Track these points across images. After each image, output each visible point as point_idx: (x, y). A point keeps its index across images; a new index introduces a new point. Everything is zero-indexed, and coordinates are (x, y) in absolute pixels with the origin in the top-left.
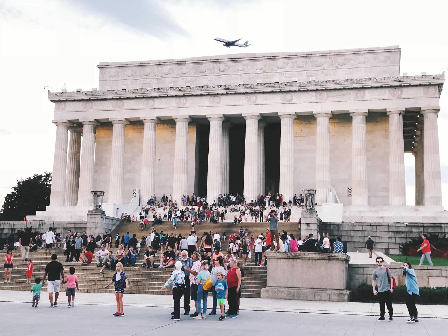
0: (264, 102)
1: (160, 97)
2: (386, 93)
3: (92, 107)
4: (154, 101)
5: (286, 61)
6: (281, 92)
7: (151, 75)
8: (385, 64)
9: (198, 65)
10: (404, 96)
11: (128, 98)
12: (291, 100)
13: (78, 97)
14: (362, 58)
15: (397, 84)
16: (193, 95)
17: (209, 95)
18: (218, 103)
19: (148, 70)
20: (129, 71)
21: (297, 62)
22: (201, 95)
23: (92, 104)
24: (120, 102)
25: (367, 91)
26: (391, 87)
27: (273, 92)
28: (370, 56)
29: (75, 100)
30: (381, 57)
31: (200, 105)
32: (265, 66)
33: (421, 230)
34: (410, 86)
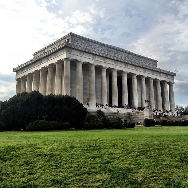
0: (139, 70)
1: (111, 59)
3: (83, 55)
4: (107, 60)
5: (133, 56)
7: (92, 46)
9: (108, 48)
11: (99, 56)
14: (150, 62)
15: (168, 73)
16: (121, 62)
17: (126, 63)
19: (91, 43)
24: (95, 56)
28: (151, 61)
31: (122, 66)
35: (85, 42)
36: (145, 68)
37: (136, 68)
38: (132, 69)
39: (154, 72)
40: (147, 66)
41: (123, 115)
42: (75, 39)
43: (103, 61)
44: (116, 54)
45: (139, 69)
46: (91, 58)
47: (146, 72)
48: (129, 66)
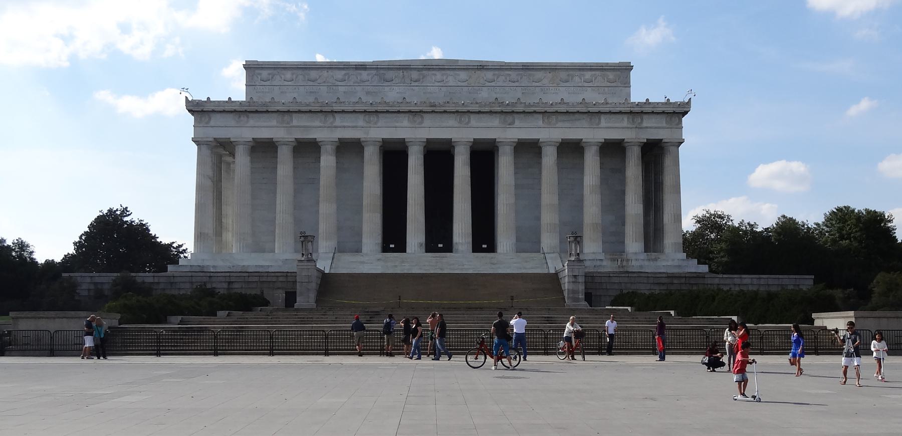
1: (343, 112)
2: (625, 121)
4: (334, 117)
6: (502, 112)
7: (319, 81)
8: (612, 84)
9: (382, 72)
10: (645, 124)
11: (300, 112)
12: (513, 123)
13: (227, 108)
14: (588, 75)
16: (388, 112)
18: (422, 123)
19: (313, 74)
20: (288, 75)
21: (509, 75)
22: (399, 112)
23: (248, 117)
24: (287, 117)
25: (603, 117)
26: (631, 112)
27: (491, 112)
28: (597, 73)
29: (224, 111)
30: (611, 75)
31: (397, 125)
32: (470, 77)
33: (683, 280)
34: (653, 112)
35: (293, 74)
36: (508, 113)
37: (465, 118)
38: (444, 124)
39: (560, 117)
40: (514, 104)
41: (281, 279)
42: (260, 74)
43: (317, 123)
44: (416, 84)
45: (474, 120)
46: (274, 123)
47: (517, 123)
48: (428, 120)
